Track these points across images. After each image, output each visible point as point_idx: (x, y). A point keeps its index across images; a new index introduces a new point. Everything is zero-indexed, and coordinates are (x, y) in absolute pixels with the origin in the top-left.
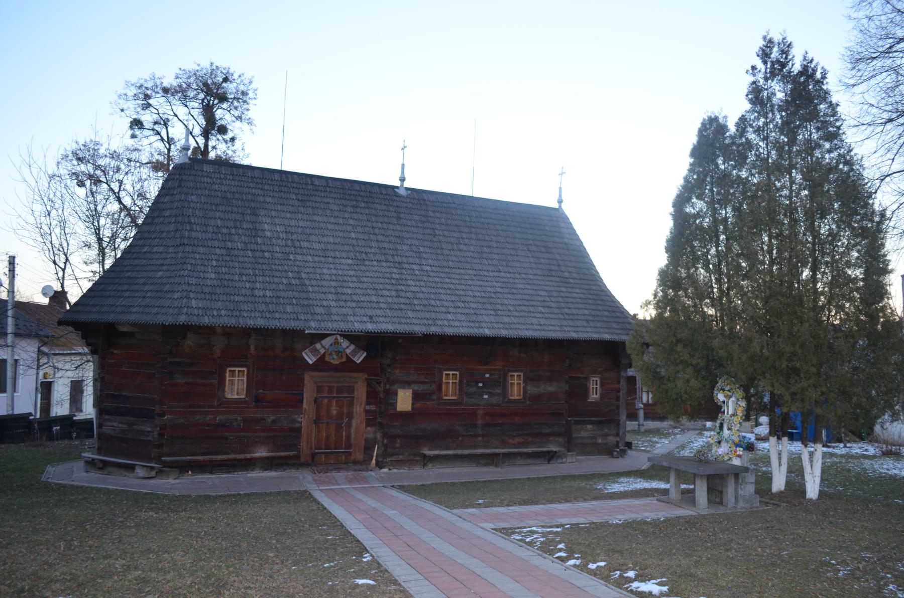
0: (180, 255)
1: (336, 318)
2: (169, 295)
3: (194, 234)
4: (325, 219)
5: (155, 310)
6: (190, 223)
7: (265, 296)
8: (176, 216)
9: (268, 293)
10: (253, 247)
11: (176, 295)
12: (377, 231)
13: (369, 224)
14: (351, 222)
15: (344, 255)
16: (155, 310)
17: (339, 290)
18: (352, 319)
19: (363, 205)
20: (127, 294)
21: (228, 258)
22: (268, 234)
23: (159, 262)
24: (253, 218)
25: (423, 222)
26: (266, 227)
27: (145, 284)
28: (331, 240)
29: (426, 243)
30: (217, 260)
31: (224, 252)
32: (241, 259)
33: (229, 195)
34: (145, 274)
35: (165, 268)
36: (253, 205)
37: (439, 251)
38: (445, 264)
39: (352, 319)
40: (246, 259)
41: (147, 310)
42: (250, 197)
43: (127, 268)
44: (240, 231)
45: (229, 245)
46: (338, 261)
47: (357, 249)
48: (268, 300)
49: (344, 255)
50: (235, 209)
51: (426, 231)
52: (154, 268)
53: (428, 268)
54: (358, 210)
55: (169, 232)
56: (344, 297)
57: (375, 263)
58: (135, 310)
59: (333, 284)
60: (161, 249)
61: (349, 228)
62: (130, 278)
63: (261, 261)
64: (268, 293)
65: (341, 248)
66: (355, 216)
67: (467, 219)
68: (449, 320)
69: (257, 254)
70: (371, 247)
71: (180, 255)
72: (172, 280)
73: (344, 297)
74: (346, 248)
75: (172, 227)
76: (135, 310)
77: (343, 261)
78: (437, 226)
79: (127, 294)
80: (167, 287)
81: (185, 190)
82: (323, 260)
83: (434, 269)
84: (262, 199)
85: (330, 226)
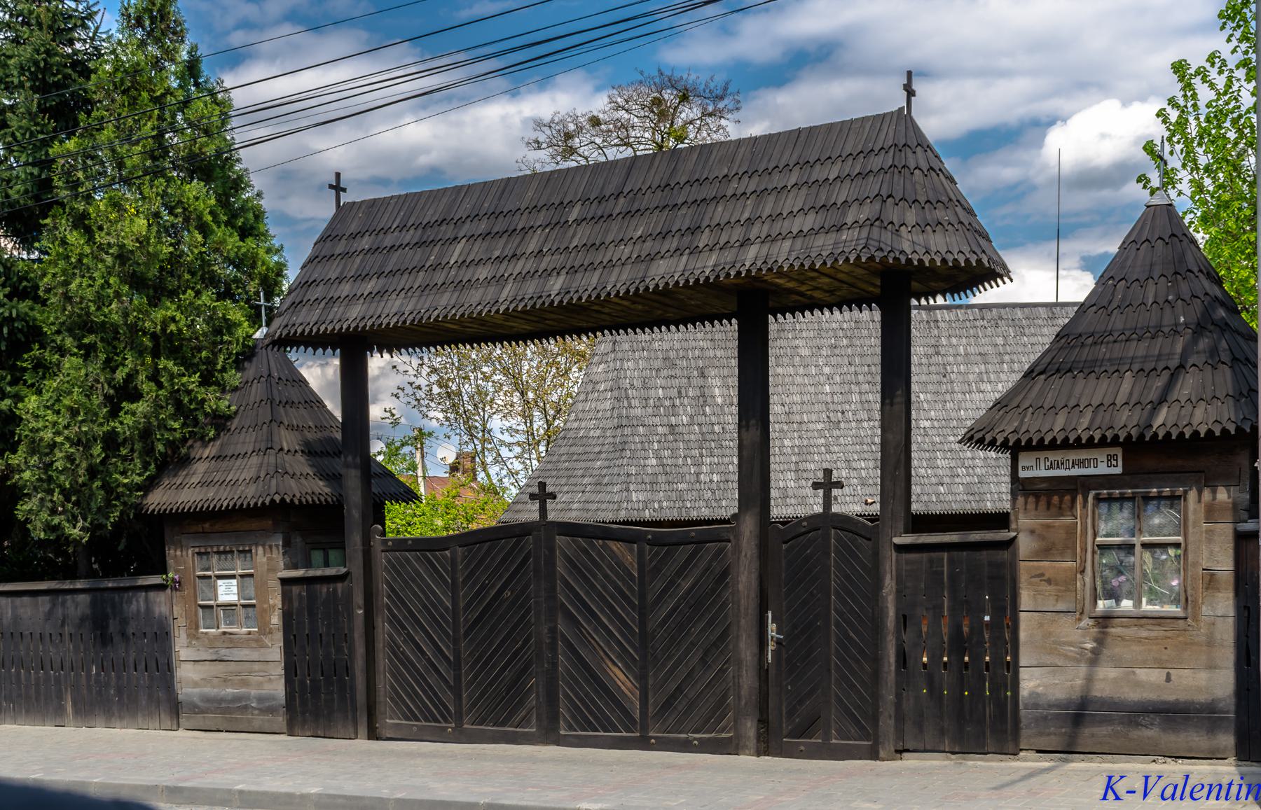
0: (618, 440)
1: (793, 501)
2: (609, 488)
3: (633, 412)
4: (791, 370)
5: (594, 506)
6: (627, 398)
7: (711, 481)
8: (612, 390)
9: (715, 478)
10: (701, 419)
11: (616, 488)
12: (861, 378)
13: (852, 369)
14: (827, 370)
15: (814, 417)
16: (594, 506)
17: (802, 466)
18: (811, 501)
19: (845, 342)
20: (566, 488)
21: (671, 438)
22: (719, 400)
23: (597, 449)
24: (700, 382)
25: (928, 356)
26: (717, 391)
27: (583, 476)
28: (797, 398)
29: (930, 387)
30: (659, 442)
31: (665, 430)
32: (686, 437)
33: (672, 354)
34: (582, 465)
35: (603, 456)
36: (701, 363)
37: (948, 397)
38: (953, 414)
39: (811, 501)
40: (693, 437)
41: (587, 506)
42: (697, 353)
43: (564, 458)
44: (686, 401)
45: (673, 420)
46: (804, 427)
47: (831, 407)
48: (714, 486)
49: (814, 417)
50: (679, 372)
51: (933, 369)
52: (592, 457)
53: (927, 424)
54: (837, 351)
55: (605, 410)
56: (805, 475)
57: (853, 424)
58: (575, 506)
59: (794, 459)
60: (598, 432)
61: (822, 379)
62: (567, 469)
63: (708, 437)
64: (715, 478)
65: (809, 407)
66: (833, 360)
67: (1000, 341)
68: (938, 494)
69: (704, 429)
70: (850, 403)
71: (618, 440)
72: (610, 471)
73: (805, 475)
74: (817, 407)
75: (608, 405)
76: (575, 506)
77: (811, 426)
78: (951, 359)
79: (566, 488)
80: (606, 480)
81: (620, 355)
82: (785, 427)
83: (936, 423)
84: (711, 353)
85: (799, 380)
